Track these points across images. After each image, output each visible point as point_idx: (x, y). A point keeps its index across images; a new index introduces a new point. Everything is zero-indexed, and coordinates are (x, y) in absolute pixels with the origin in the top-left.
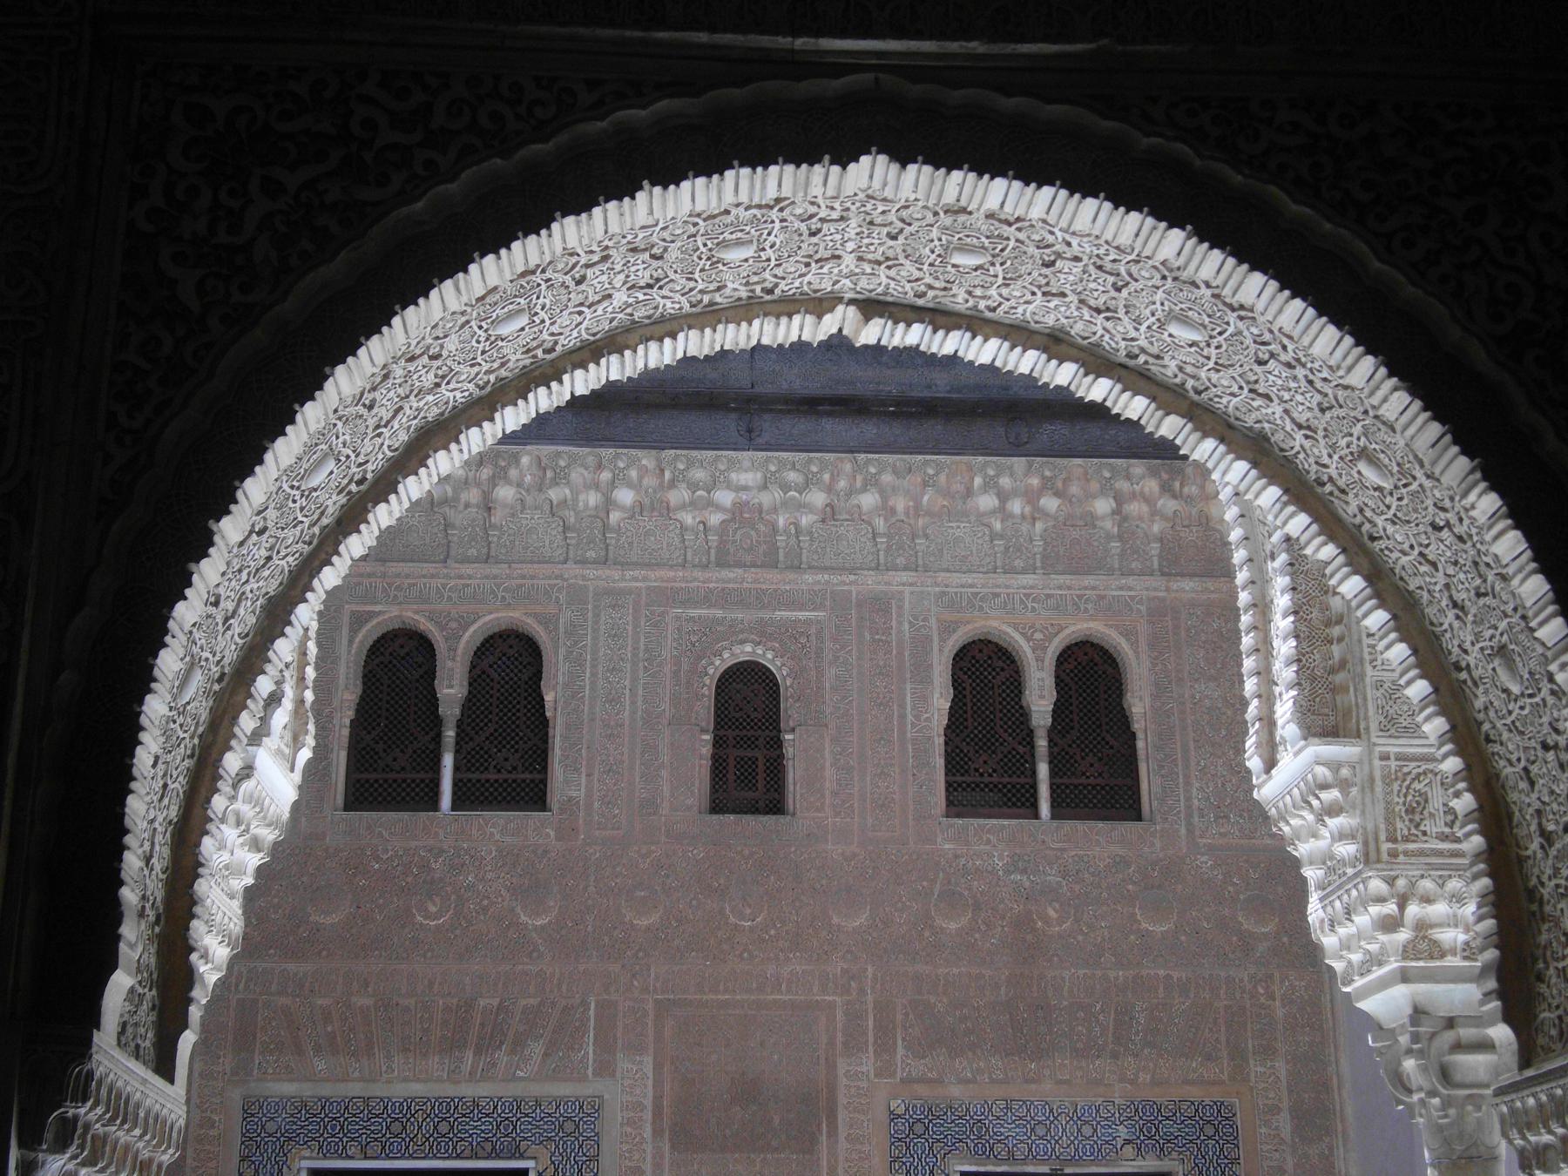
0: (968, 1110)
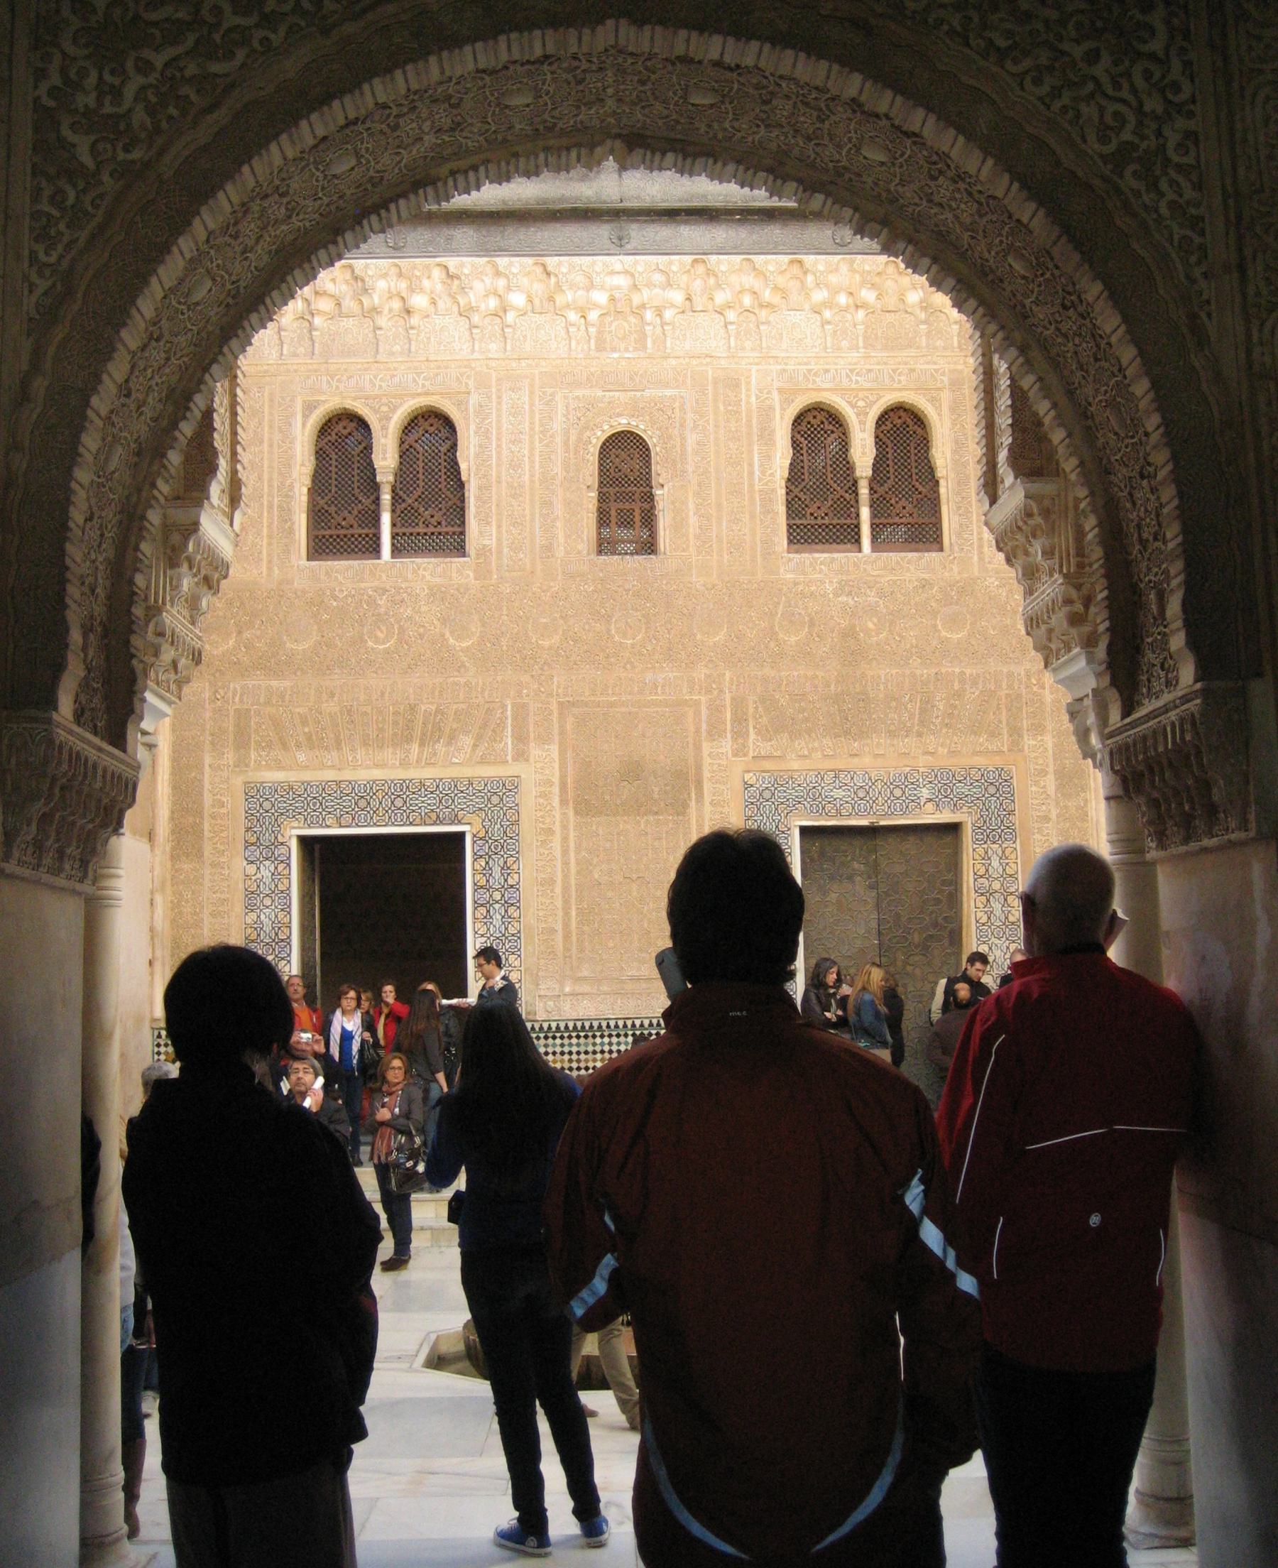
0: (805, 779)
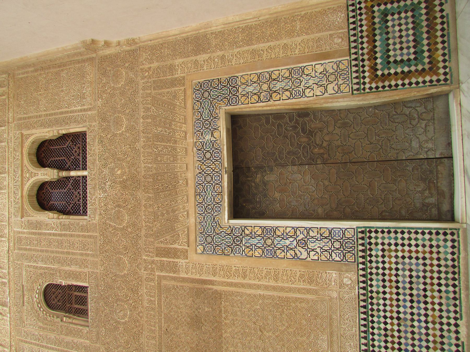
0: (200, 214)
